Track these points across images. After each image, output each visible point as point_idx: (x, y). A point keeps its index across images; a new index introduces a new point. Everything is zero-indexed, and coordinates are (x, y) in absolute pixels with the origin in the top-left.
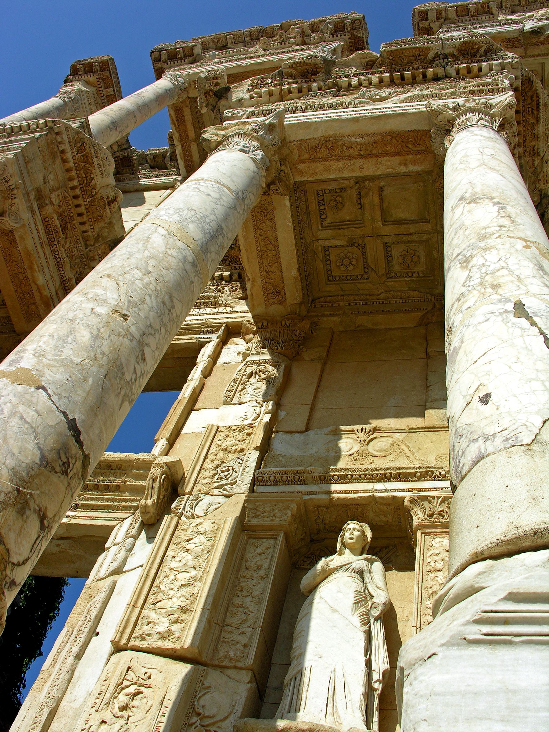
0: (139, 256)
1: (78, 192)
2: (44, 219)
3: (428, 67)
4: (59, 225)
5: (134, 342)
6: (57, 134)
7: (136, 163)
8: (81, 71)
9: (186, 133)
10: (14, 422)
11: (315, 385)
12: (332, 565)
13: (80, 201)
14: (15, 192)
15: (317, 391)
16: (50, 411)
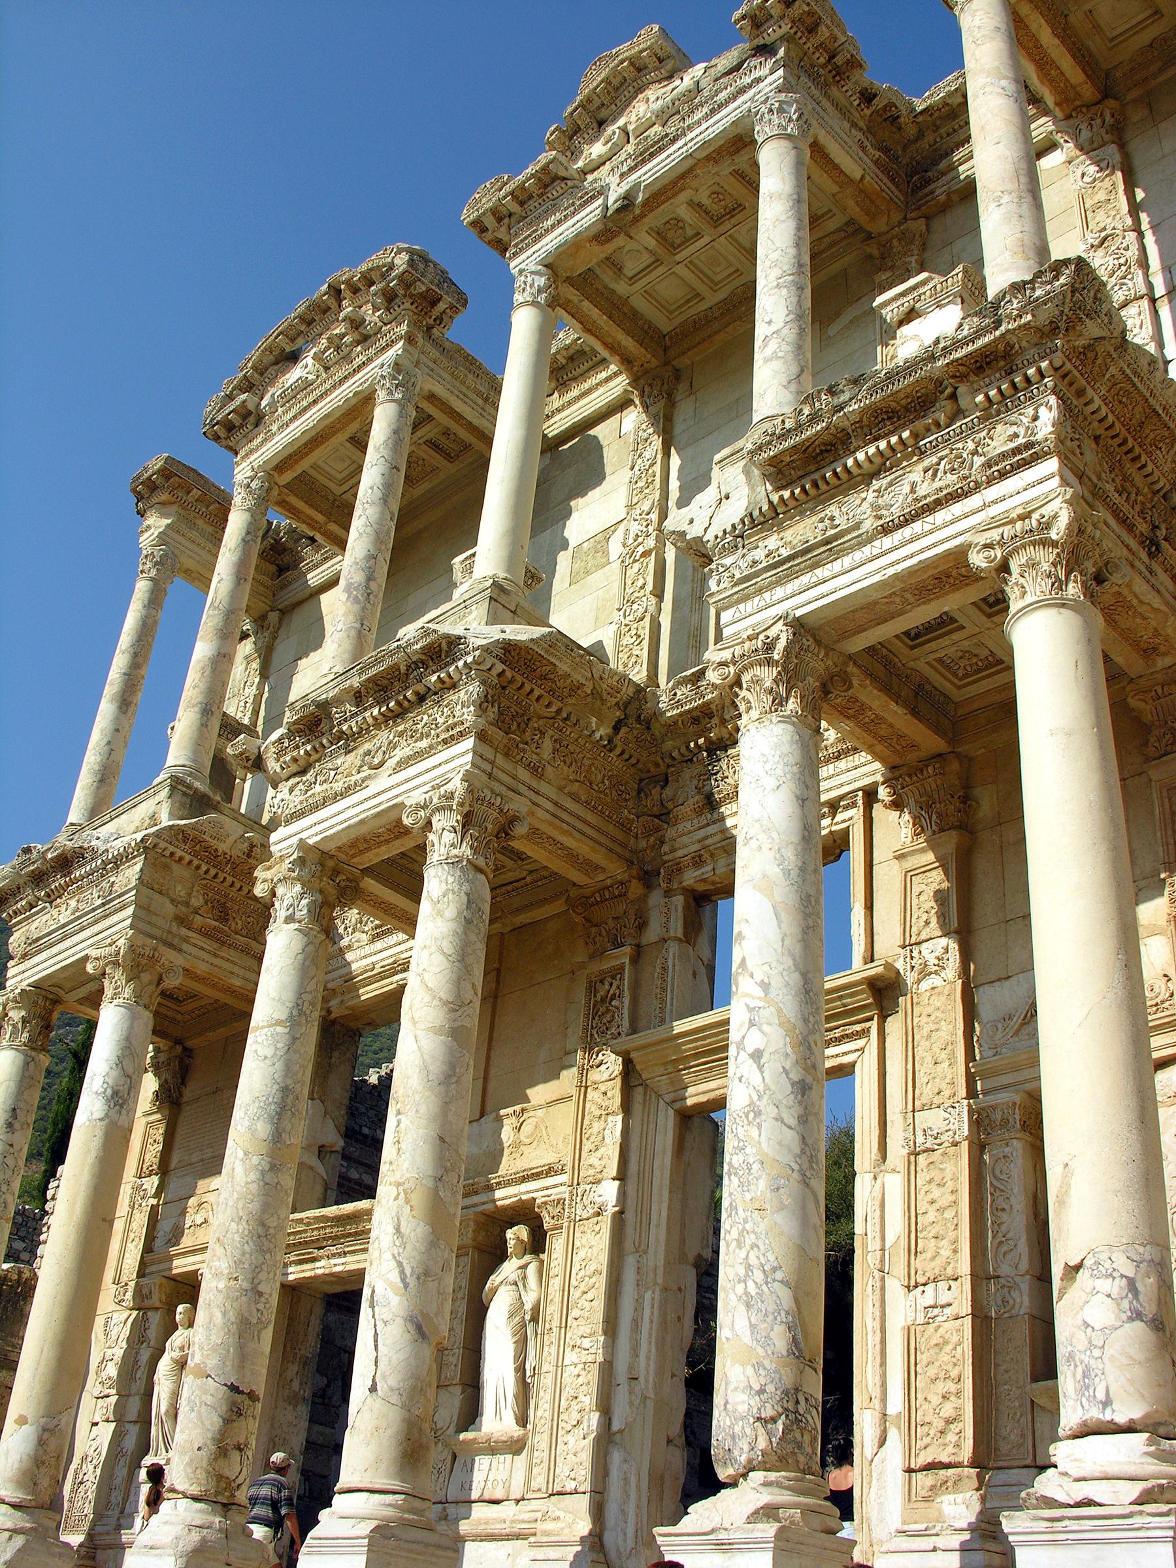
0: (231, 1203)
1: (213, 872)
2: (200, 932)
3: (407, 688)
4: (217, 924)
5: (249, 1293)
6: (155, 846)
7: (290, 545)
8: (146, 494)
9: (312, 519)
10: (204, 1409)
11: (486, 1044)
12: (496, 1283)
13: (221, 876)
14: (156, 954)
15: (489, 1049)
16: (218, 1389)
